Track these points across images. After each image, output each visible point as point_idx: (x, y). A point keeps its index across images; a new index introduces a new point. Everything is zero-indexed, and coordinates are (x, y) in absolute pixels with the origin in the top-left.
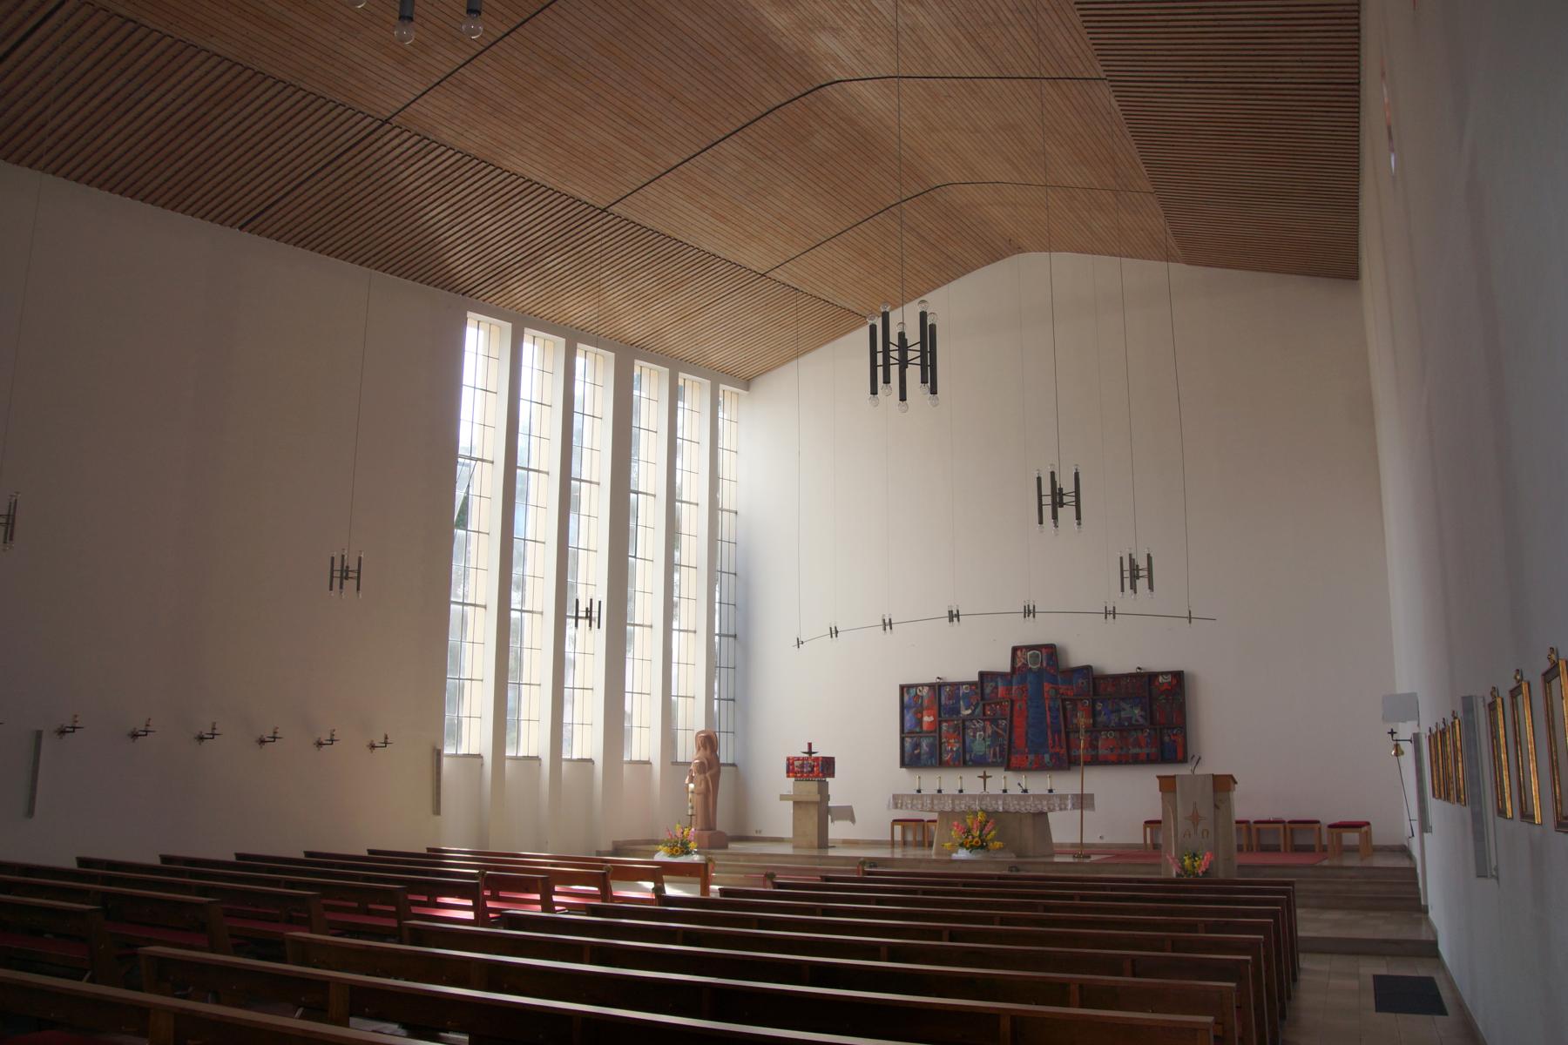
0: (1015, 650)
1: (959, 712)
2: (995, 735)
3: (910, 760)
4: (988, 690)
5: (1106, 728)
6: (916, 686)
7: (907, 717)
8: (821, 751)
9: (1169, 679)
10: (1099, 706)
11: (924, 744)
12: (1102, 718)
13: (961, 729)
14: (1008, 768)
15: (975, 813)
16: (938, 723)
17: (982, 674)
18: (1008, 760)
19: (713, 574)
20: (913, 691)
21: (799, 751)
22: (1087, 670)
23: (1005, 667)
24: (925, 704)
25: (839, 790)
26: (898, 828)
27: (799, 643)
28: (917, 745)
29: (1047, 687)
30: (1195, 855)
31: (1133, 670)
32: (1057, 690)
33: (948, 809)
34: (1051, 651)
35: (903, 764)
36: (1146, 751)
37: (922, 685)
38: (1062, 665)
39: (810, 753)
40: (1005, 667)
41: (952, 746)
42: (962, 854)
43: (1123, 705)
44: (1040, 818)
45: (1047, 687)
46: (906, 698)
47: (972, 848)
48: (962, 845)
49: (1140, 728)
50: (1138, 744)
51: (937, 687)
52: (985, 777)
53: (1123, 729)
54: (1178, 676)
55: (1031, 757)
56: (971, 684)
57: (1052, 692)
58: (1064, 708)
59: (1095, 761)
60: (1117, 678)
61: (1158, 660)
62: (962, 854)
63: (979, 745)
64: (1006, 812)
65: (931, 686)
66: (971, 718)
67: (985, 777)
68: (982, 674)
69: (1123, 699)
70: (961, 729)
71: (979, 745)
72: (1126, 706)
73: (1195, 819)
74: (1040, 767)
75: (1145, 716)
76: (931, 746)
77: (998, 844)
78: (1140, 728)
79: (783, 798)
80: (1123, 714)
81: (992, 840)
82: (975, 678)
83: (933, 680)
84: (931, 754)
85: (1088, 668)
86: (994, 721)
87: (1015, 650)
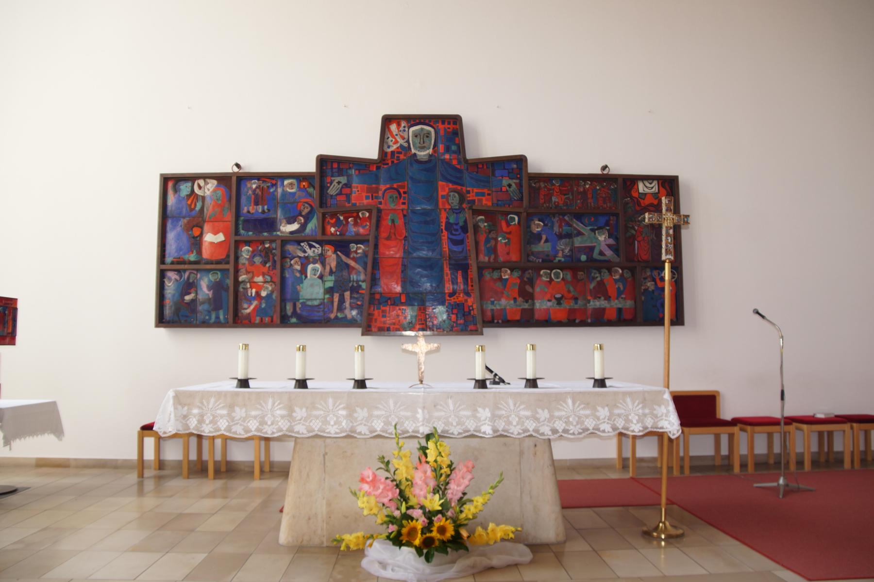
0: (387, 120)
1: (270, 224)
4: (333, 190)
5: (549, 263)
6: (191, 178)
7: (171, 236)
9: (654, 187)
10: (537, 226)
12: (543, 247)
13: (277, 259)
17: (323, 161)
20: (185, 188)
23: (372, 153)
24: (209, 211)
26: (150, 442)
28: (189, 286)
29: (443, 188)
31: (595, 169)
32: (462, 199)
33: (332, 430)
34: (450, 128)
35: (162, 320)
36: (616, 304)
37: (206, 177)
41: (260, 286)
43: (578, 225)
46: (171, 200)
48: (397, 540)
49: (608, 266)
50: (601, 291)
51: (233, 183)
53: (581, 267)
57: (454, 199)
58: (476, 228)
59: (528, 320)
60: (569, 182)
63: (312, 289)
65: (222, 179)
66: (296, 239)
68: (323, 161)
69: (579, 217)
70: (277, 259)
71: (312, 289)
72: (585, 230)
76: (217, 288)
78: (608, 266)
80: (578, 242)
82: (310, 167)
83: (226, 167)
84: (216, 303)
85: (520, 161)
86: (342, 246)
87: (387, 120)
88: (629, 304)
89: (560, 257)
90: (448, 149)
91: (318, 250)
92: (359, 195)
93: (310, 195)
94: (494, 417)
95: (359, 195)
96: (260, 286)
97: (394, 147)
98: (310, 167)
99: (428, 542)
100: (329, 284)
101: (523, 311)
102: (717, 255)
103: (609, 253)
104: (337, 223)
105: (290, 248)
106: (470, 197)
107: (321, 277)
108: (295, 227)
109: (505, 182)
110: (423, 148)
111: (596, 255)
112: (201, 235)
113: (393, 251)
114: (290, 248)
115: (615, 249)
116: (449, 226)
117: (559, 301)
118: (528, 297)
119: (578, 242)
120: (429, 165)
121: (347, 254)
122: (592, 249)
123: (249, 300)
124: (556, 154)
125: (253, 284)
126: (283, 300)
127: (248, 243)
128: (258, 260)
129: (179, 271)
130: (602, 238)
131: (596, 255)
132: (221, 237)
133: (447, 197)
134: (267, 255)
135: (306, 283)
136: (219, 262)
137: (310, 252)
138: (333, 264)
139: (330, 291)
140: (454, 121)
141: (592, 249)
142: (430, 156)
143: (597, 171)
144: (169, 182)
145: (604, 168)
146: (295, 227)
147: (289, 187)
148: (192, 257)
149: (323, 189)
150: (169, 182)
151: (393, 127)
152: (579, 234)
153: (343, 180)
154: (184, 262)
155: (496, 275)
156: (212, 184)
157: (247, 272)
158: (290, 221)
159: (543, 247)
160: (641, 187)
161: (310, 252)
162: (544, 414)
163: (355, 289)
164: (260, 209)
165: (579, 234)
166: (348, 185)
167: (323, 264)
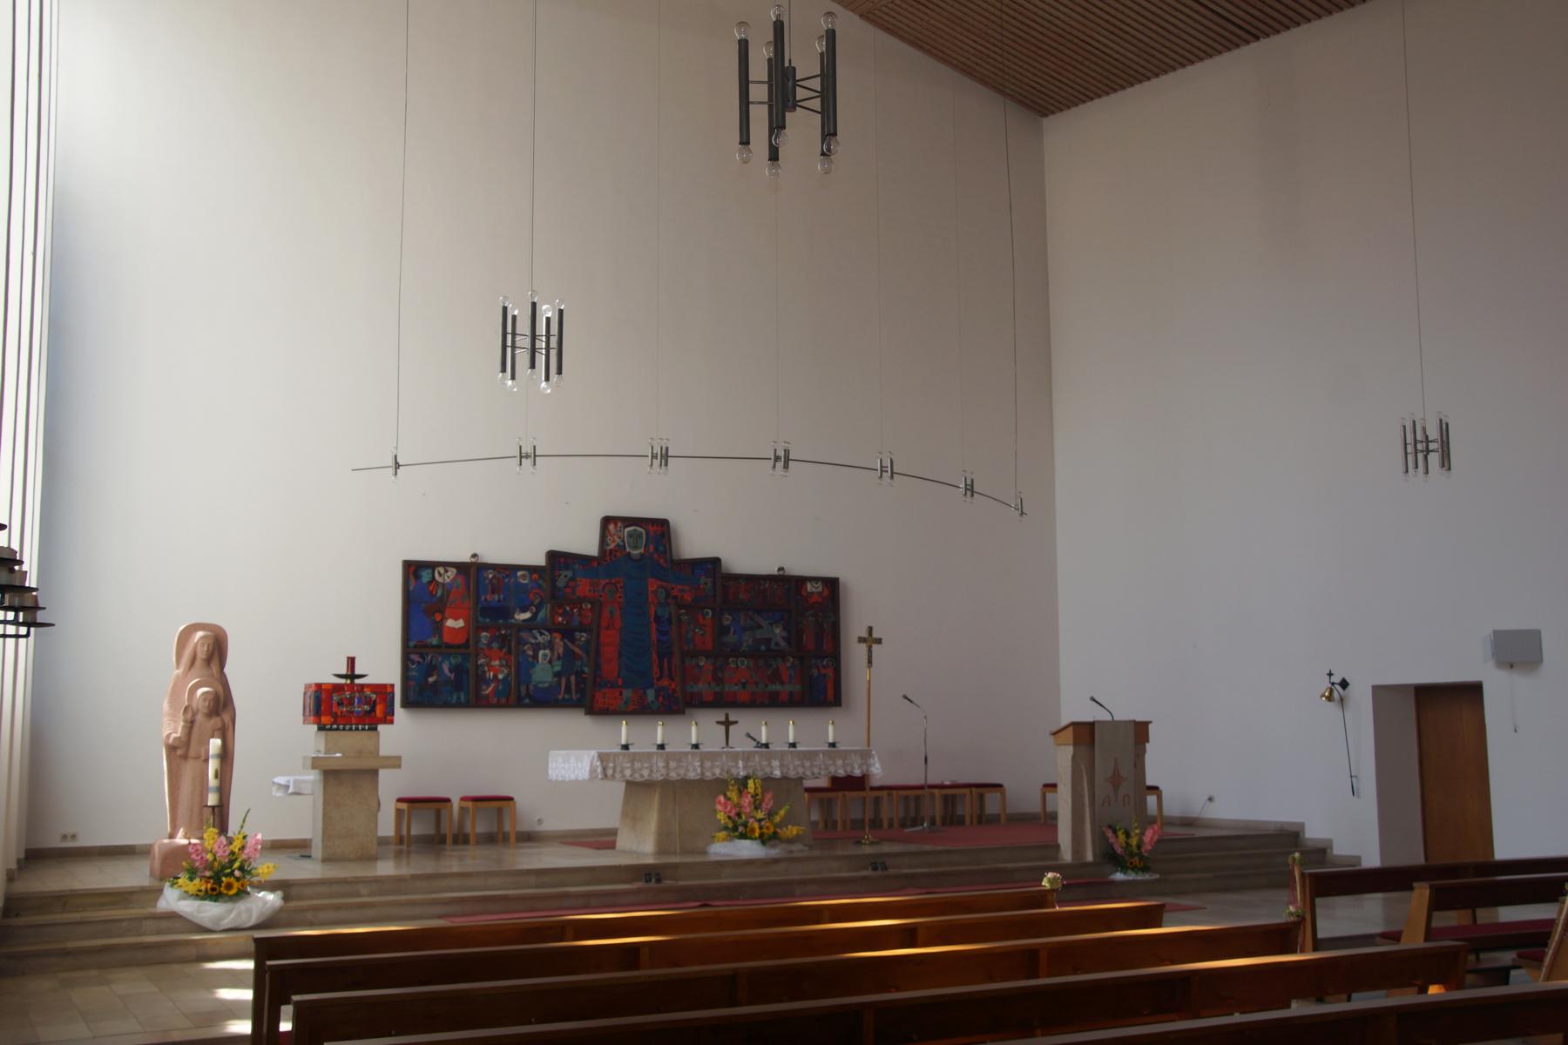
0: (607, 521)
1: (503, 612)
2: (569, 657)
4: (561, 583)
5: (735, 652)
6: (432, 565)
9: (819, 587)
10: (727, 620)
11: (446, 667)
12: (731, 638)
14: (592, 711)
15: (742, 783)
16: (478, 632)
17: (553, 556)
21: (329, 672)
22: (712, 565)
28: (432, 669)
31: (772, 569)
33: (692, 775)
34: (659, 530)
36: (789, 688)
37: (446, 565)
39: (352, 676)
40: (586, 542)
41: (497, 669)
42: (748, 849)
47: (764, 840)
48: (743, 836)
50: (776, 677)
51: (472, 571)
52: (727, 724)
54: (832, 584)
55: (627, 693)
56: (531, 569)
57: (662, 595)
58: (679, 620)
60: (753, 581)
61: (802, 558)
63: (543, 673)
64: (784, 778)
65: (461, 567)
66: (528, 626)
67: (727, 724)
70: (511, 641)
71: (543, 673)
72: (764, 623)
73: (1116, 780)
74: (640, 710)
75: (781, 637)
80: (759, 634)
81: (783, 824)
82: (540, 561)
83: (465, 557)
84: (458, 685)
85: (716, 561)
86: (568, 633)
87: (607, 521)
88: (798, 688)
89: (744, 647)
90: (656, 550)
91: (547, 637)
92: (583, 587)
93: (540, 587)
94: (782, 766)
97: (612, 546)
98: (540, 561)
99: (762, 835)
100: (557, 668)
101: (716, 694)
103: (783, 644)
104: (564, 614)
105: (523, 635)
106: (674, 593)
107: (550, 662)
108: (527, 615)
109: (703, 580)
110: (635, 548)
111: (773, 646)
112: (443, 620)
114: (523, 635)
115: (788, 640)
116: (657, 619)
117: (744, 685)
119: (759, 634)
121: (573, 641)
122: (769, 640)
123: (488, 683)
124: (748, 556)
125: (491, 668)
126: (518, 683)
127: (485, 629)
128: (495, 645)
129: (422, 656)
130: (777, 631)
131: (773, 646)
132: (460, 623)
133: (655, 592)
134: (504, 641)
135: (538, 668)
136: (459, 647)
137: (540, 639)
138: (561, 650)
139: (557, 675)
140: (663, 523)
141: (769, 640)
142: (642, 555)
143: (775, 571)
144: (413, 569)
145: (781, 569)
146: (527, 615)
147: (523, 579)
148: (435, 641)
149: (554, 581)
150: (413, 569)
151: (611, 527)
152: (760, 627)
153: (569, 574)
154: (426, 646)
155: (694, 662)
156: (452, 572)
157: (486, 656)
158: (524, 611)
159: (731, 638)
160: (809, 587)
161: (540, 639)
162: (807, 764)
163: (579, 674)
164: (496, 597)
165: (760, 627)
166: (573, 579)
167: (552, 650)
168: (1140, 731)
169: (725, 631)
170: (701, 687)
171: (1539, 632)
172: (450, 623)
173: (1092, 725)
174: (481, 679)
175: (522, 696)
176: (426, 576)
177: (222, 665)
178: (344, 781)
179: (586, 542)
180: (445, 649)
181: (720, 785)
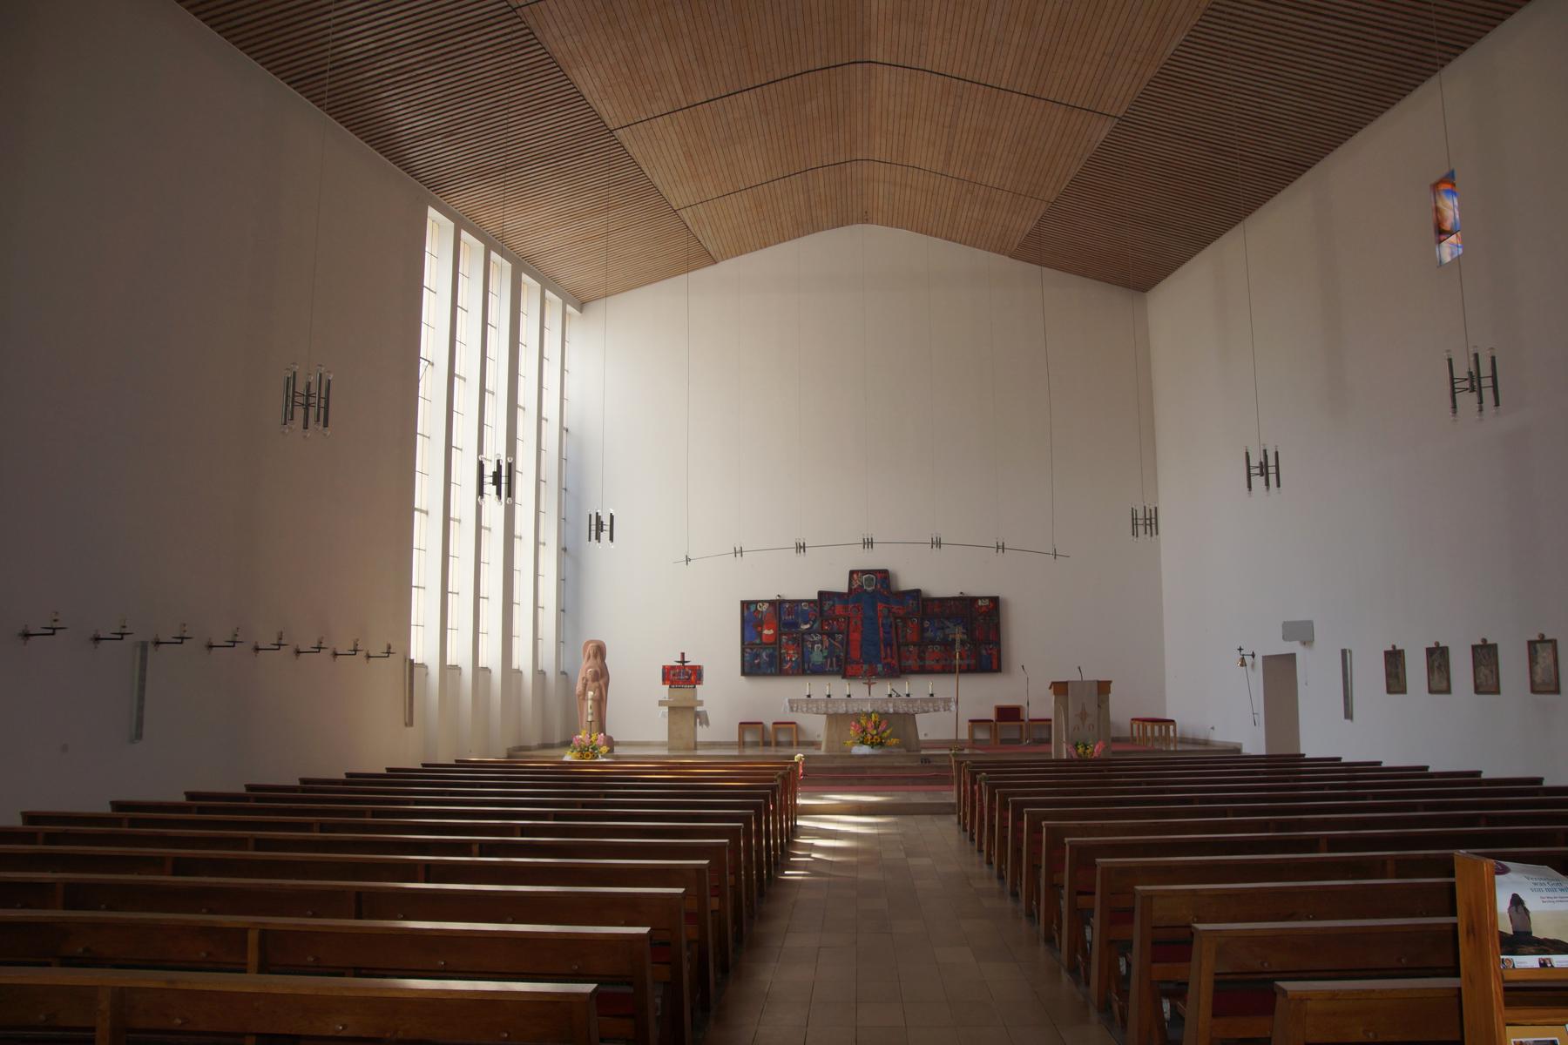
0: (852, 573)
1: (795, 625)
2: (831, 648)
3: (750, 668)
5: (933, 642)
6: (756, 602)
8: (692, 660)
9: (987, 602)
10: (927, 624)
12: (929, 634)
13: (800, 642)
14: (844, 677)
15: (869, 715)
17: (821, 594)
18: (843, 668)
19: (562, 489)
21: (673, 660)
22: (916, 593)
25: (707, 694)
27: (688, 560)
28: (757, 656)
29: (881, 607)
30: (1086, 746)
31: (957, 594)
33: (842, 710)
34: (883, 576)
35: (744, 673)
38: (893, 589)
39: (683, 662)
40: (841, 586)
41: (792, 655)
42: (865, 750)
44: (909, 718)
45: (881, 607)
47: (872, 745)
51: (777, 605)
54: (995, 601)
55: (865, 667)
56: (810, 602)
57: (885, 611)
59: (923, 671)
60: (942, 601)
61: (976, 585)
62: (865, 750)
63: (817, 656)
64: (896, 713)
66: (809, 631)
68: (821, 594)
70: (800, 642)
71: (817, 656)
73: (1083, 716)
75: (966, 632)
76: (770, 656)
77: (894, 741)
79: (661, 703)
82: (815, 597)
83: (773, 597)
84: (770, 664)
85: (918, 591)
86: (831, 635)
87: (852, 573)
95: (839, 609)
96: (792, 655)
98: (815, 597)
102: (1024, 636)
113: (855, 636)
118: (922, 659)
120: (873, 595)
140: (885, 572)
144: (745, 605)
147: (805, 607)
150: (745, 605)
156: (765, 607)
159: (929, 634)
168: (1104, 687)
169: (924, 630)
170: (910, 662)
171: (1310, 623)
172: (766, 632)
173: (1066, 683)
174: (782, 661)
175: (805, 669)
176: (753, 608)
177: (603, 659)
178: (684, 713)
179: (841, 586)
180: (764, 645)
181: (856, 716)
